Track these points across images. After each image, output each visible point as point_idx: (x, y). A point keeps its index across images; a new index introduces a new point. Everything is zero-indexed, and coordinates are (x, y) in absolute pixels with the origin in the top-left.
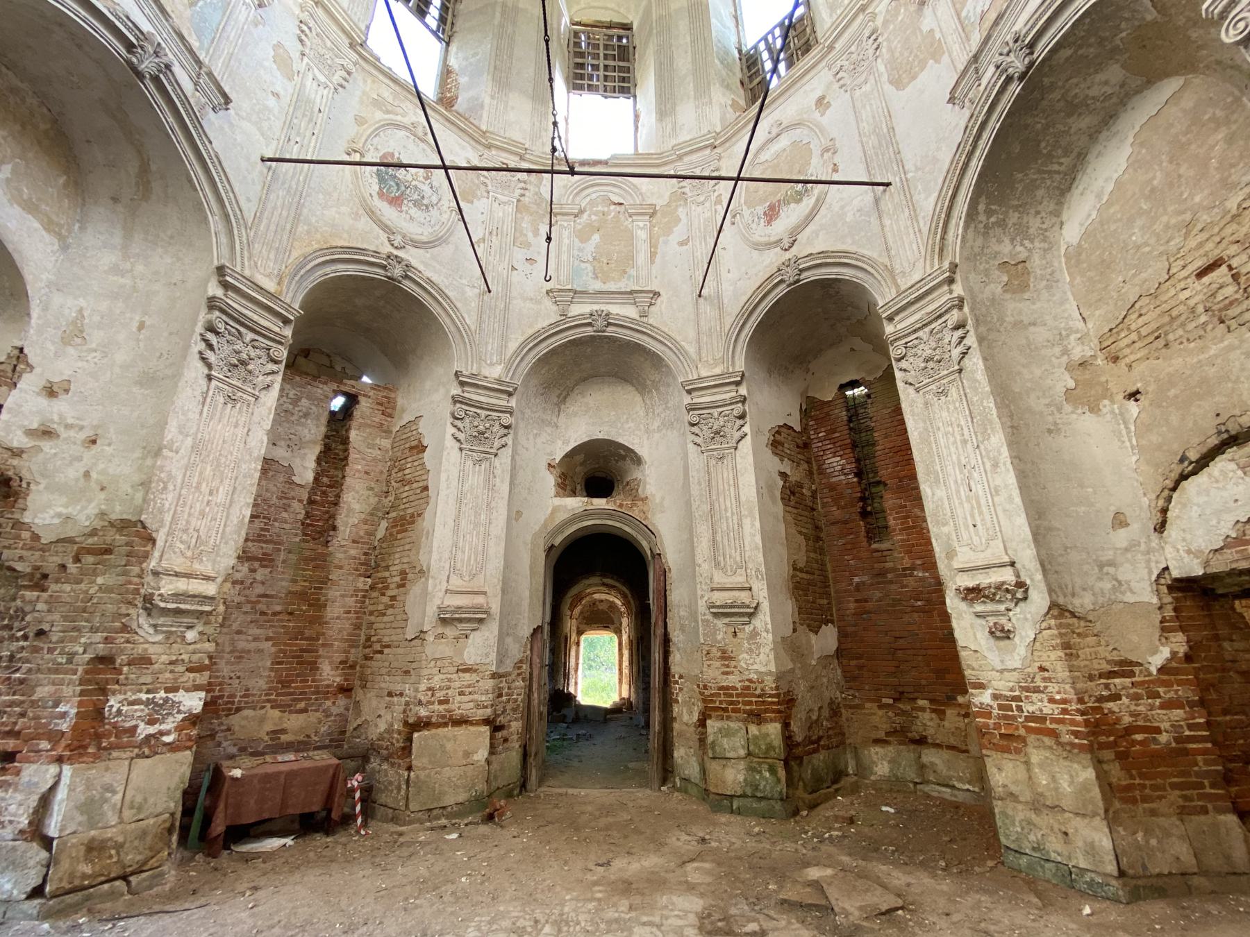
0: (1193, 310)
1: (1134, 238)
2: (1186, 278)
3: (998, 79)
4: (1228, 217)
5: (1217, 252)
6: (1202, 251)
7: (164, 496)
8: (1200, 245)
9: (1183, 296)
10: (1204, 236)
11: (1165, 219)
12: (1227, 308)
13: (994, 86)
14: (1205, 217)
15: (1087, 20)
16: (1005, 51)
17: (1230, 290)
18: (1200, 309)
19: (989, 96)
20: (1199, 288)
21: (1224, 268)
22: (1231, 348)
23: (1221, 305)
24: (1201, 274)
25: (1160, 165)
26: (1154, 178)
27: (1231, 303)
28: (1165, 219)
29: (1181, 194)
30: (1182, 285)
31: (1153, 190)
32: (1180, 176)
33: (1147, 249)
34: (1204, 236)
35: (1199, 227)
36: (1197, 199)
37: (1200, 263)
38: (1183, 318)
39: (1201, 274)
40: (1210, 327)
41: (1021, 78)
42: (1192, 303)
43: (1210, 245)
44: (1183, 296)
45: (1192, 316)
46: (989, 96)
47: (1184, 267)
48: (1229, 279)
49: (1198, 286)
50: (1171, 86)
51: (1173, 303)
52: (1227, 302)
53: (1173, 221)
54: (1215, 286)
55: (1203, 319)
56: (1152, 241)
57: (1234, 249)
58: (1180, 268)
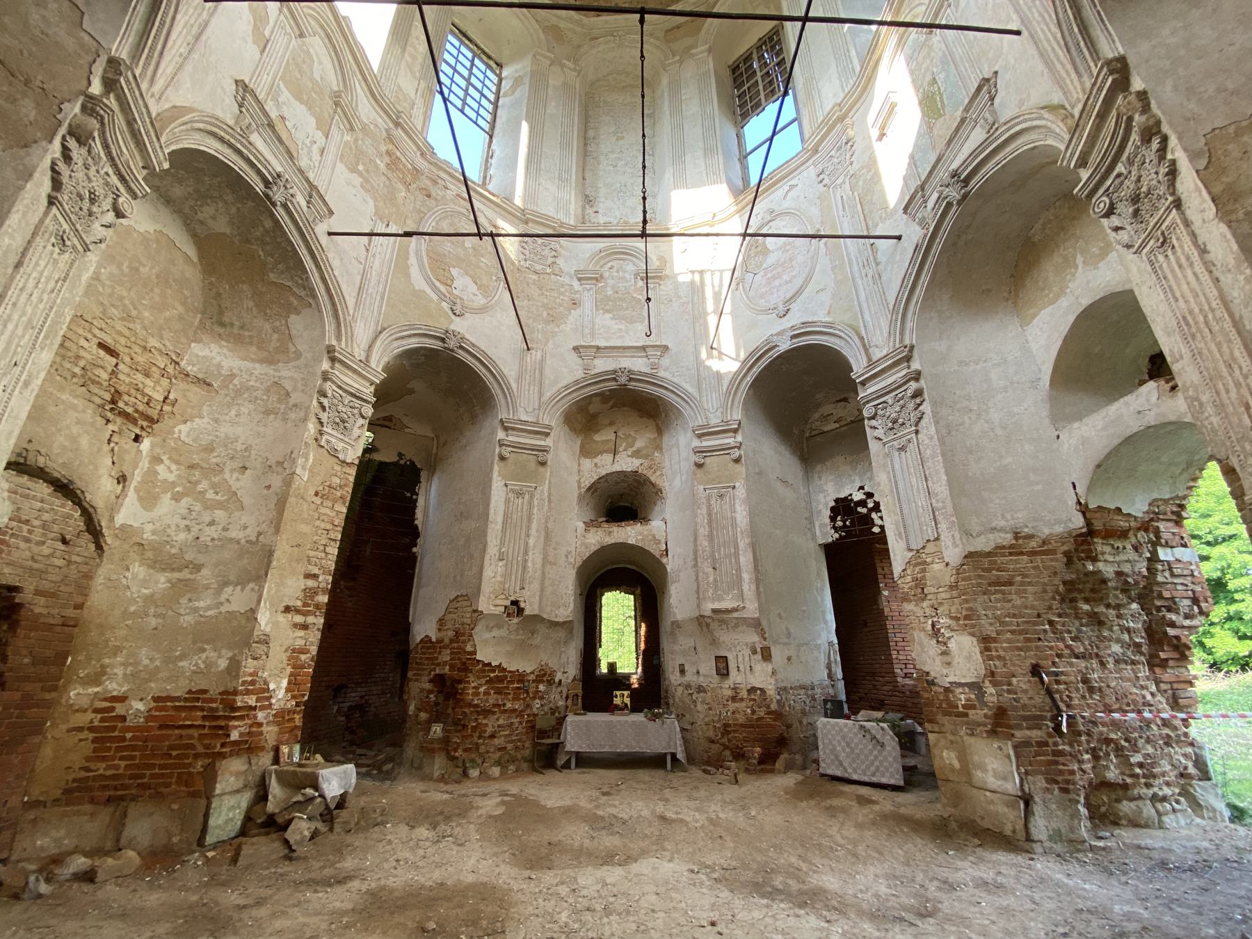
0: (78, 357)
1: (103, 270)
2: (95, 336)
3: (270, 173)
4: (143, 343)
5: (121, 349)
6: (117, 337)
7: (1206, 414)
8: (119, 333)
9: (83, 342)
10: (126, 332)
11: (125, 294)
12: (93, 382)
13: (266, 168)
14: (138, 327)
15: (289, 249)
16: (288, 186)
17: (105, 376)
18: (82, 363)
19: (260, 161)
20: (94, 352)
21: (114, 361)
22: (74, 407)
23: (93, 377)
24: (101, 345)
25: (153, 267)
26: (144, 266)
27: (98, 383)
28: (125, 294)
29: (144, 298)
30: (89, 336)
31: (137, 269)
32: (152, 290)
33: (100, 289)
34: (126, 332)
35: (131, 326)
36: (146, 314)
37: (109, 341)
38: (69, 354)
39: (101, 345)
40: (75, 380)
41: (267, 196)
42: (82, 353)
43: (123, 341)
44: (83, 342)
45: (73, 360)
46: (260, 161)
47: (101, 329)
48: (110, 370)
49: (95, 349)
50: (192, 252)
51: (74, 337)
52: (97, 379)
53: (127, 302)
54: (100, 363)
55: (77, 370)
56: (109, 291)
57: (127, 359)
58: (99, 326)
